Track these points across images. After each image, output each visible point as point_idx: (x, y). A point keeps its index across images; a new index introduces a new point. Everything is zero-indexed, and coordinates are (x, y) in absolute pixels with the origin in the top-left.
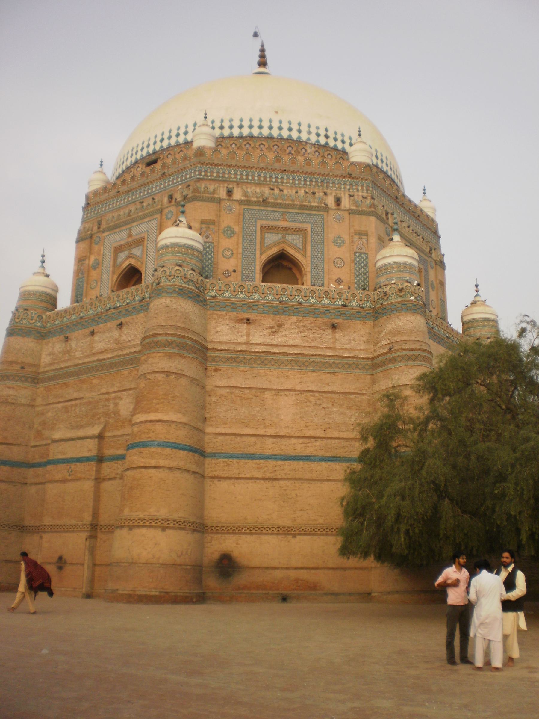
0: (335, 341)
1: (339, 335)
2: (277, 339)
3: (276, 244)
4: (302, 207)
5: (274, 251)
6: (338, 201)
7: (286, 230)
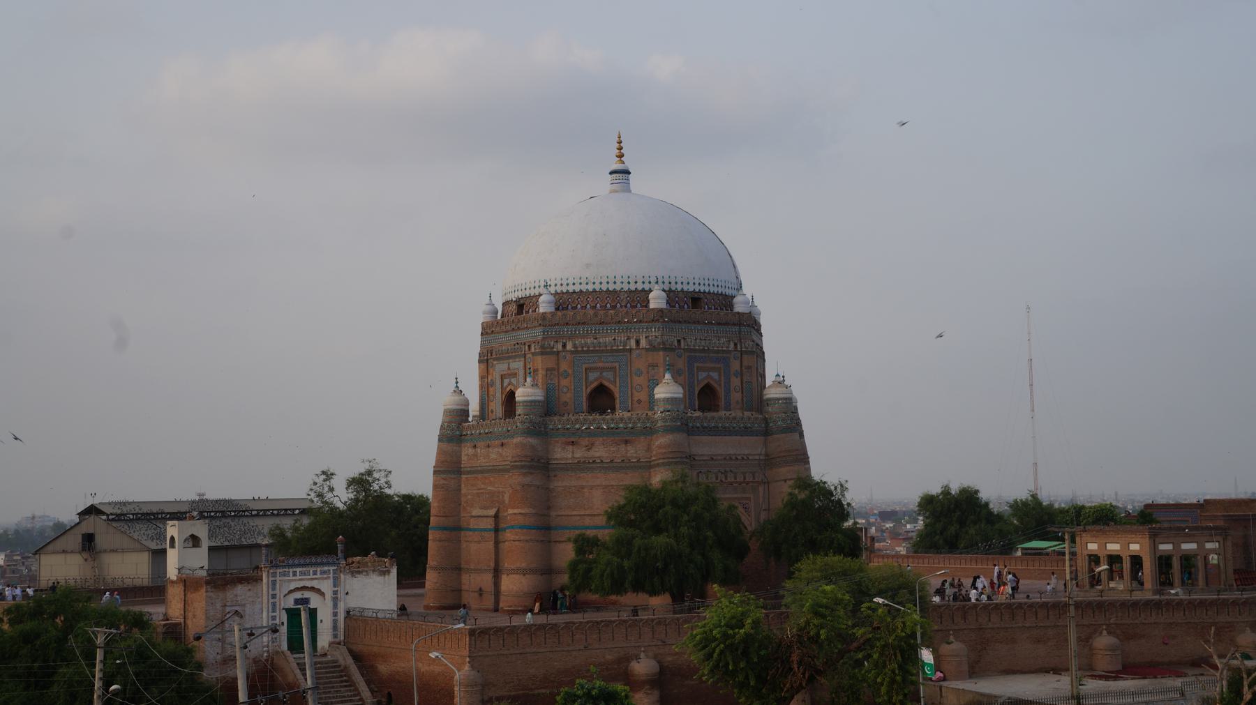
0: (627, 451)
1: (629, 448)
2: (591, 453)
3: (596, 380)
4: (612, 351)
5: (595, 384)
6: (638, 342)
7: (602, 369)
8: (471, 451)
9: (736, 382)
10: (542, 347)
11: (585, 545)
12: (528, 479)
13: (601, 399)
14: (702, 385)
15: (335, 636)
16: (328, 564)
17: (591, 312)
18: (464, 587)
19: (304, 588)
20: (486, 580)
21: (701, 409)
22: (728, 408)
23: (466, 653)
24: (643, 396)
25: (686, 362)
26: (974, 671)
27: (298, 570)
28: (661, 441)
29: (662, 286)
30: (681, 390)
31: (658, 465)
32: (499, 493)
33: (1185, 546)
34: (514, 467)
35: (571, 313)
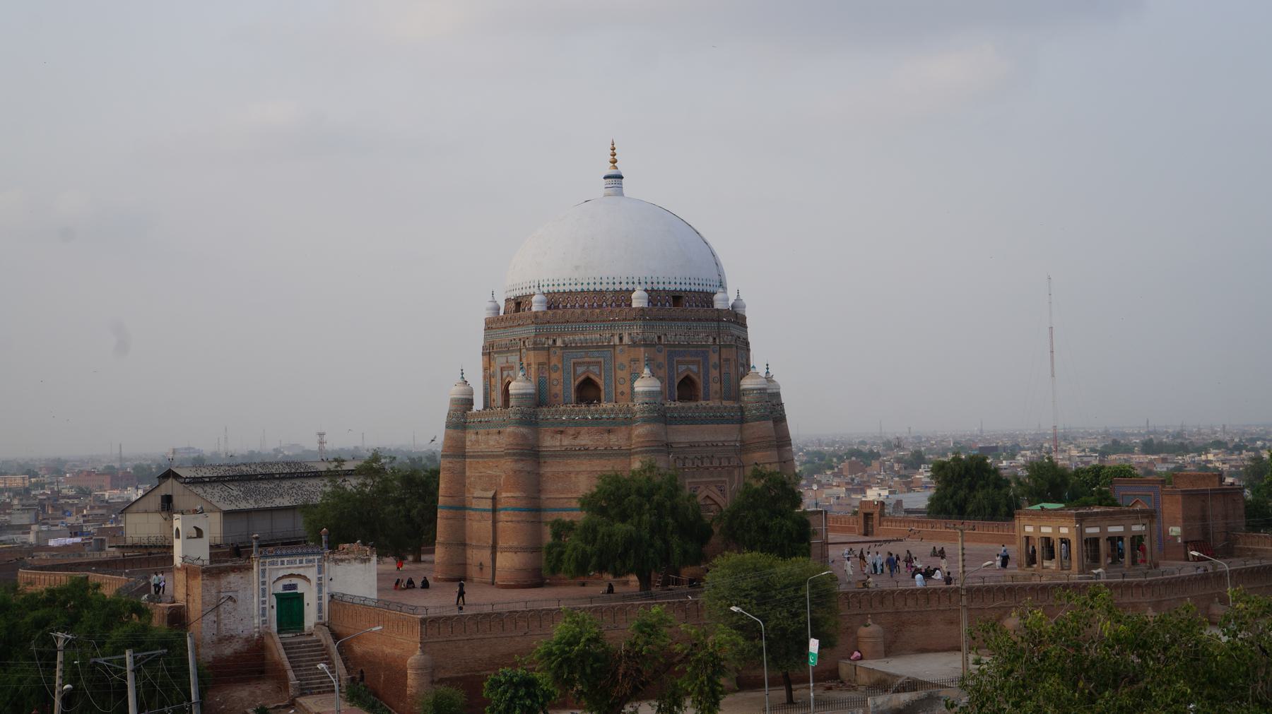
2: (577, 442)
4: (598, 347)
6: (621, 339)
8: (474, 437)
9: (714, 373)
10: (535, 343)
11: (561, 529)
12: (519, 466)
13: (588, 391)
15: (320, 618)
16: (313, 554)
17: (579, 311)
18: (469, 561)
19: (291, 575)
20: (485, 556)
21: (681, 399)
22: (706, 398)
23: (418, 639)
24: (623, 388)
25: (661, 354)
26: (891, 650)
27: (285, 559)
28: (640, 430)
29: (644, 286)
30: (658, 383)
31: (636, 453)
32: (490, 481)
33: (1112, 529)
34: (507, 455)
35: (560, 312)
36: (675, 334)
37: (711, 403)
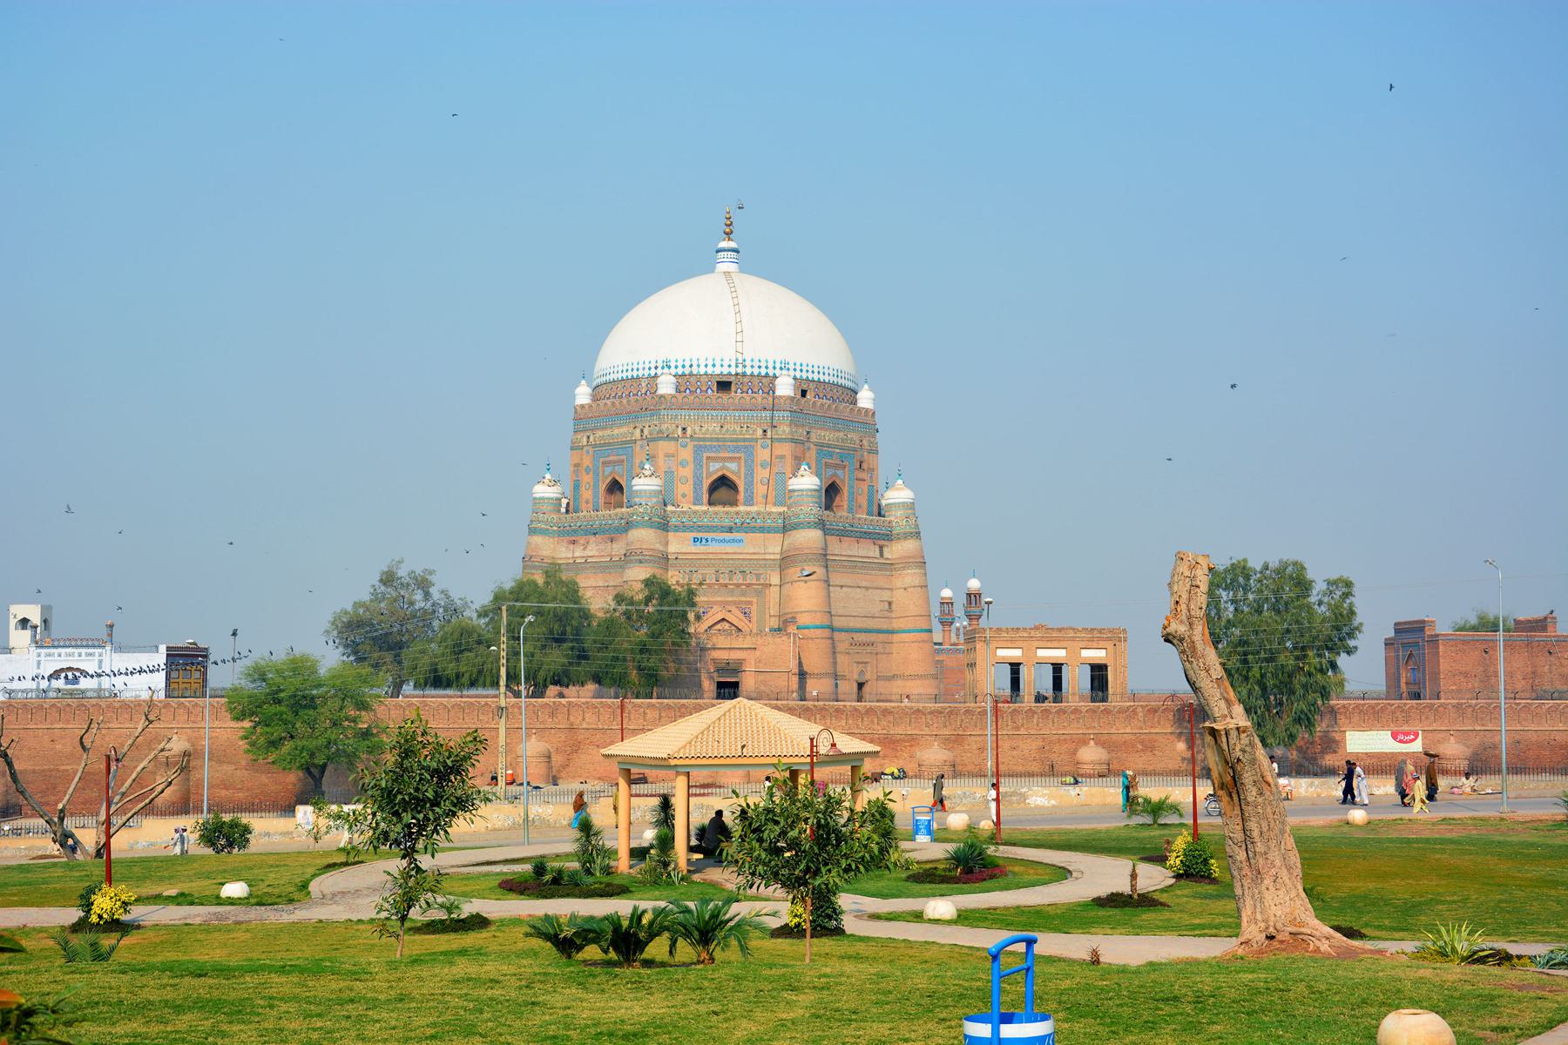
9: (762, 474)
14: (715, 477)
22: (750, 501)
36: (709, 426)
37: (754, 509)
